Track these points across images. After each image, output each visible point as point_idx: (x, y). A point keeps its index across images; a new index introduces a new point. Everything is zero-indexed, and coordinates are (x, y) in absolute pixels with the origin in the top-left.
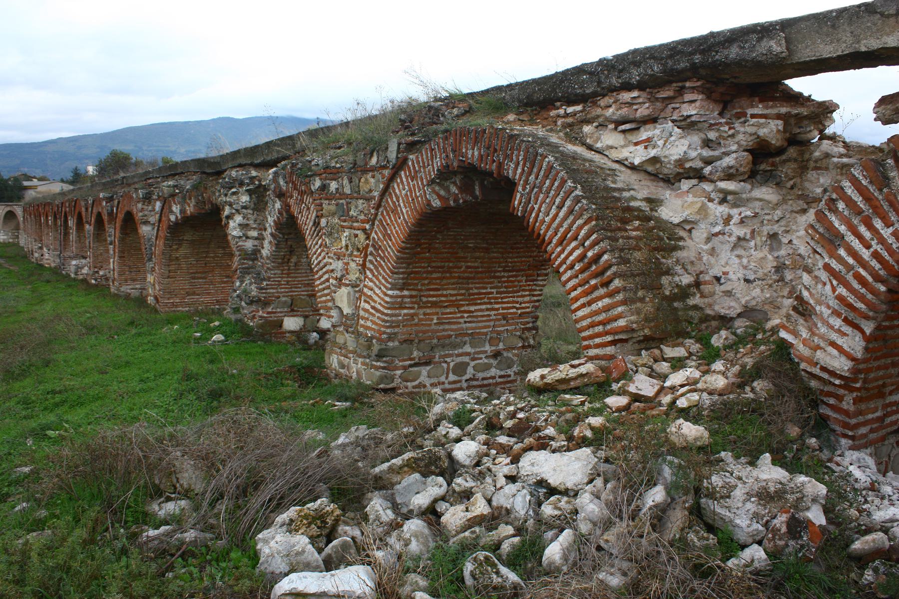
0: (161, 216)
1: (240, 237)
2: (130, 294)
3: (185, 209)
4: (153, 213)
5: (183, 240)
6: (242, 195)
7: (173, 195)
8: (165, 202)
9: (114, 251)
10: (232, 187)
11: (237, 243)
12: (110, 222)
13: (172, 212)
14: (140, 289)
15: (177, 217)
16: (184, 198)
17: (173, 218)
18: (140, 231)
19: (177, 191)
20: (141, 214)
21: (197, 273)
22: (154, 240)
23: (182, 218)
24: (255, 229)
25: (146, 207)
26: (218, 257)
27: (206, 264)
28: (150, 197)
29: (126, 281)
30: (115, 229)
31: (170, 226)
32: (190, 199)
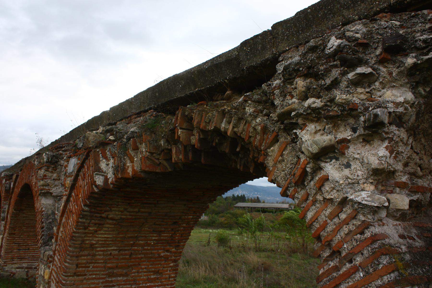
0: (76, 179)
1: (375, 210)
2: (14, 274)
3: (125, 165)
4: (57, 183)
5: (107, 218)
6: (384, 86)
7: (103, 144)
8: (88, 156)
9: (5, 227)
10: (361, 62)
11: (366, 226)
12: (6, 199)
13: (98, 170)
14: (27, 268)
15: (106, 179)
16: (124, 148)
17: (99, 180)
18: (37, 205)
19: (111, 138)
20: (42, 182)
21: (117, 267)
22: (58, 217)
23: (117, 179)
24: (402, 186)
25: (50, 174)
26: (149, 245)
27: (131, 255)
28: (57, 162)
29: (13, 259)
30: (9, 205)
31: (93, 193)
32: (136, 149)
